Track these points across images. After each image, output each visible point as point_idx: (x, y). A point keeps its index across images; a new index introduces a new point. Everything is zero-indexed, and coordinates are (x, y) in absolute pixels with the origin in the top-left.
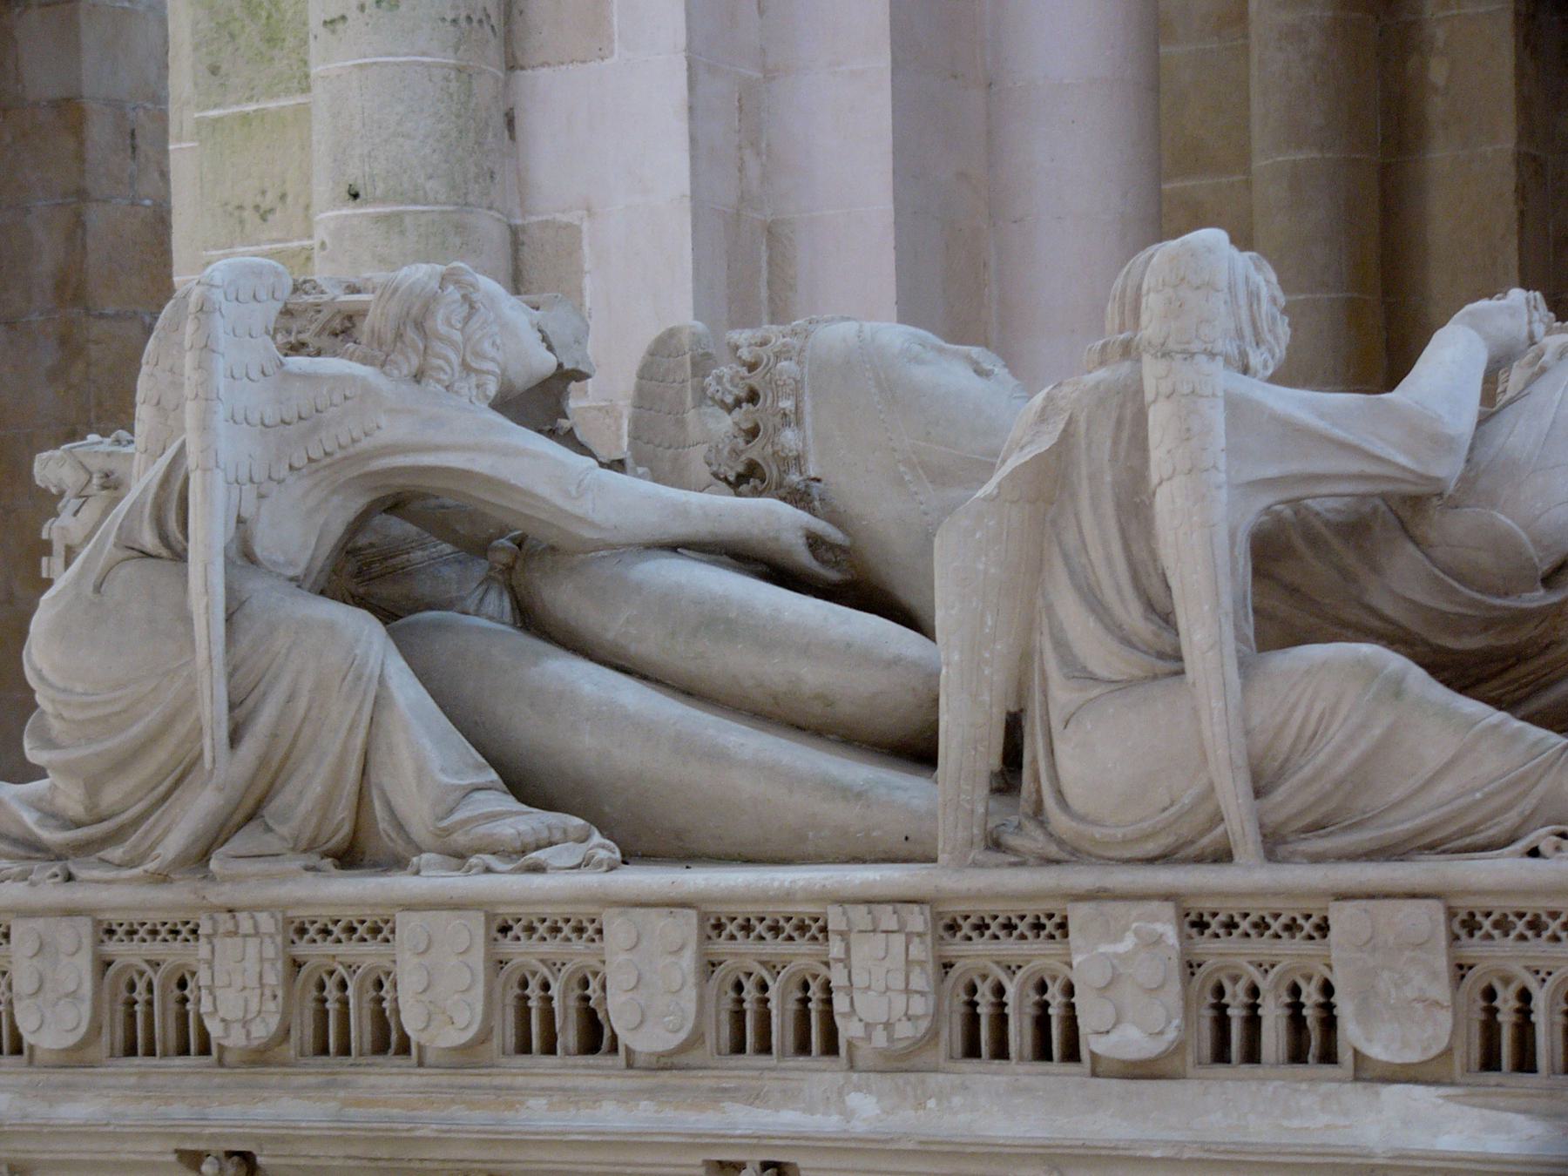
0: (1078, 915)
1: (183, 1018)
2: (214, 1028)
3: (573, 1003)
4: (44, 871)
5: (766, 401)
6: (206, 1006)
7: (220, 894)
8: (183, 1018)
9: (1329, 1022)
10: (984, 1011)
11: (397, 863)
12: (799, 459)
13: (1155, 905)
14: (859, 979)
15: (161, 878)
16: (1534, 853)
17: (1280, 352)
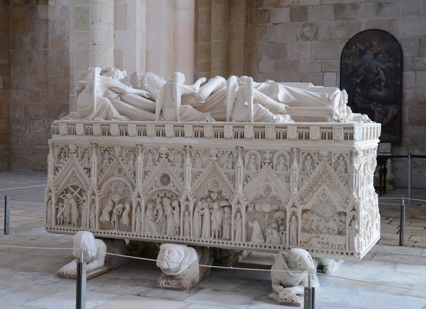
0: (166, 125)
1: (91, 132)
2: (94, 133)
3: (125, 132)
4: (78, 119)
5: (143, 81)
6: (93, 131)
7: (94, 121)
8: (91, 132)
9: (184, 134)
10: (158, 133)
11: (110, 120)
12: (146, 87)
13: (171, 125)
14: (148, 130)
15: (90, 120)
16: (199, 121)
17: (184, 82)
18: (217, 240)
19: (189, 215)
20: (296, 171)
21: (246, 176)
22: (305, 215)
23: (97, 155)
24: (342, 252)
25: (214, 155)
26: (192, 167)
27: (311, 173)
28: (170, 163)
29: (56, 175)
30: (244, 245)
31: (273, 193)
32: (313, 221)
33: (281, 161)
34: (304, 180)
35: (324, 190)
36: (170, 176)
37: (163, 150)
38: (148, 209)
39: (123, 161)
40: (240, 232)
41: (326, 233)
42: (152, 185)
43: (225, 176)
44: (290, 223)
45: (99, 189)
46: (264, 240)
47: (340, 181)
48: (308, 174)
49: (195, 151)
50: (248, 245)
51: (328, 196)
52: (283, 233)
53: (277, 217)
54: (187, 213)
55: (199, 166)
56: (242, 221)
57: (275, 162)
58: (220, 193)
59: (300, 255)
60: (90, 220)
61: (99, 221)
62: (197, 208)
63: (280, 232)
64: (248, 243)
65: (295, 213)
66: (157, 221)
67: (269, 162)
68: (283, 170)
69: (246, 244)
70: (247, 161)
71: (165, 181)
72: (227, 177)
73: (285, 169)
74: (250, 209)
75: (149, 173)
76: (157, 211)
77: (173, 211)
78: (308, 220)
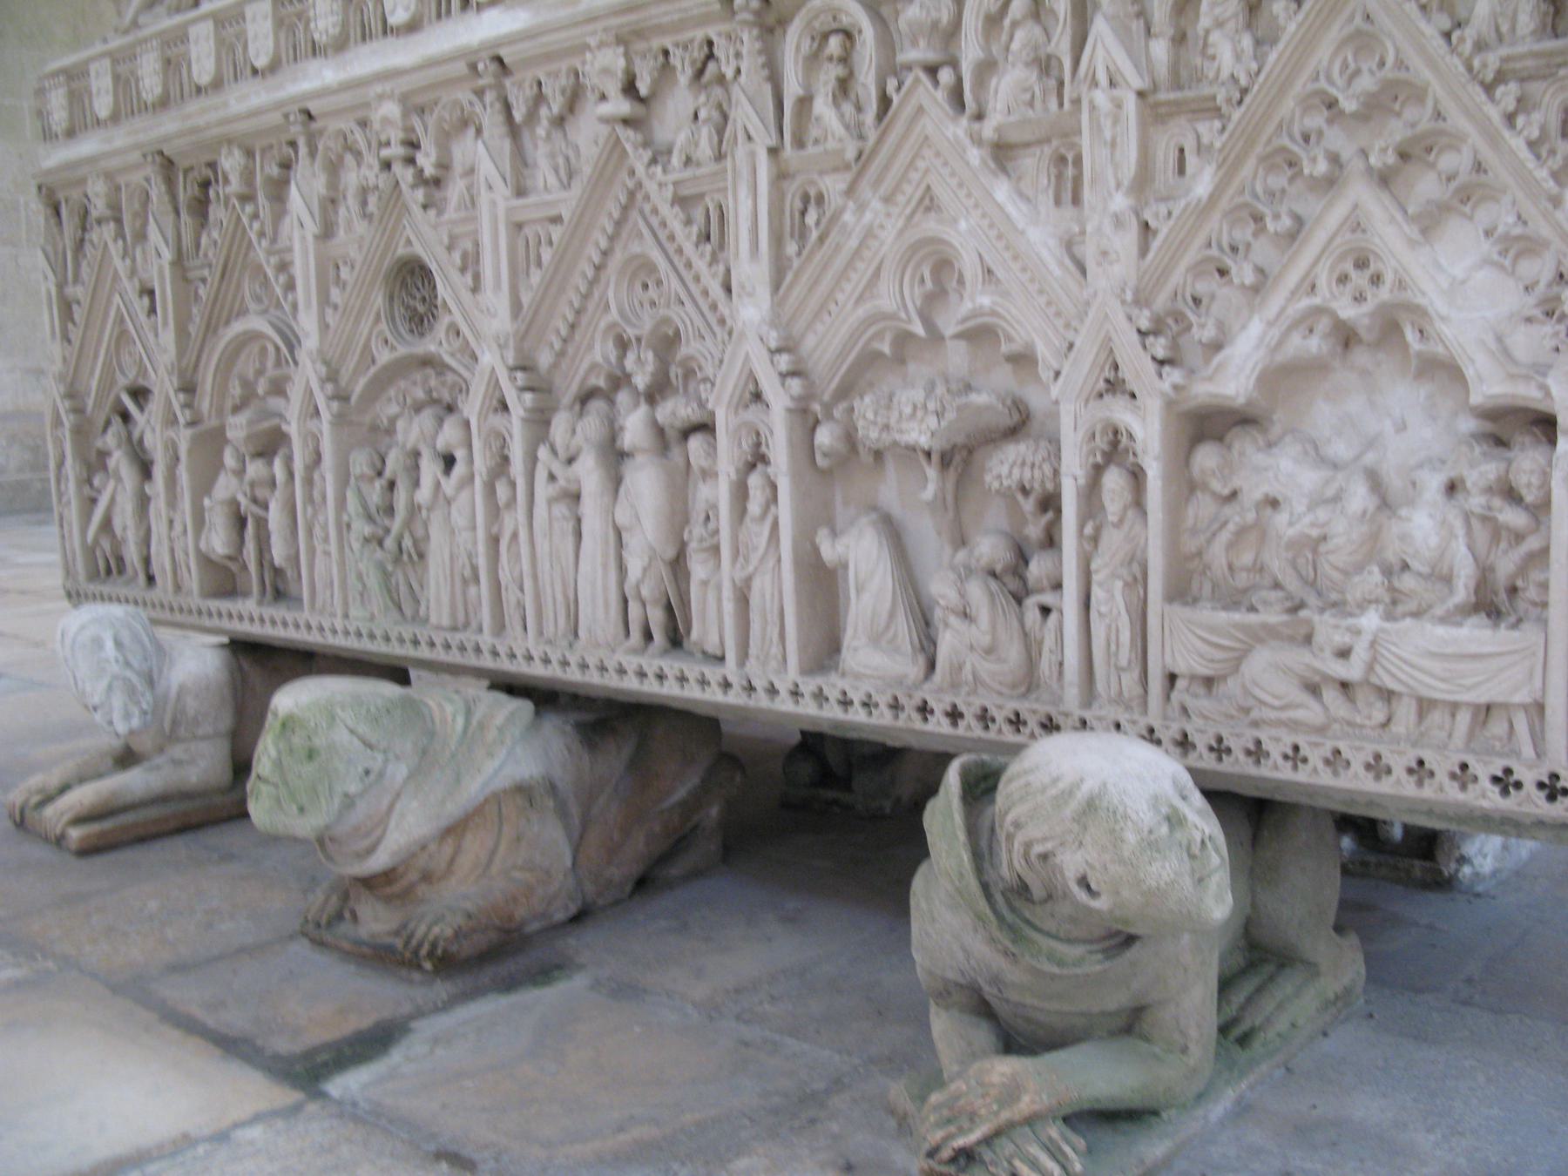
18: (652, 662)
19: (513, 500)
20: (1117, 92)
21: (806, 199)
22: (1206, 458)
23: (177, 212)
24: (1508, 771)
25: (613, 88)
26: (507, 192)
27: (1244, 91)
28: (420, 194)
29: (69, 341)
30: (796, 693)
31: (977, 299)
32: (1274, 503)
33: (1020, 35)
34: (1191, 161)
35: (1358, 227)
36: (433, 267)
37: (386, 121)
38: (352, 480)
39: (256, 225)
40: (768, 605)
41: (1377, 601)
42: (369, 339)
43: (673, 218)
44: (1089, 530)
45: (189, 388)
46: (922, 661)
47: (1494, 114)
48: (1220, 99)
49: (529, 91)
50: (820, 696)
51: (1389, 278)
52: (1045, 611)
53: (1006, 483)
54: (502, 491)
55: (552, 180)
56: (775, 525)
57: (970, 51)
58: (667, 343)
59: (1086, 788)
60: (172, 551)
61: (198, 550)
62: (543, 453)
63: (1031, 602)
64: (819, 680)
65: (1124, 440)
66: (389, 543)
67: (931, 56)
68: (1031, 104)
69: (808, 686)
70: (792, 88)
71: (421, 309)
72: (688, 222)
73: (1045, 92)
74: (825, 437)
75: (345, 273)
76: (392, 485)
77: (443, 480)
78: (1234, 495)
